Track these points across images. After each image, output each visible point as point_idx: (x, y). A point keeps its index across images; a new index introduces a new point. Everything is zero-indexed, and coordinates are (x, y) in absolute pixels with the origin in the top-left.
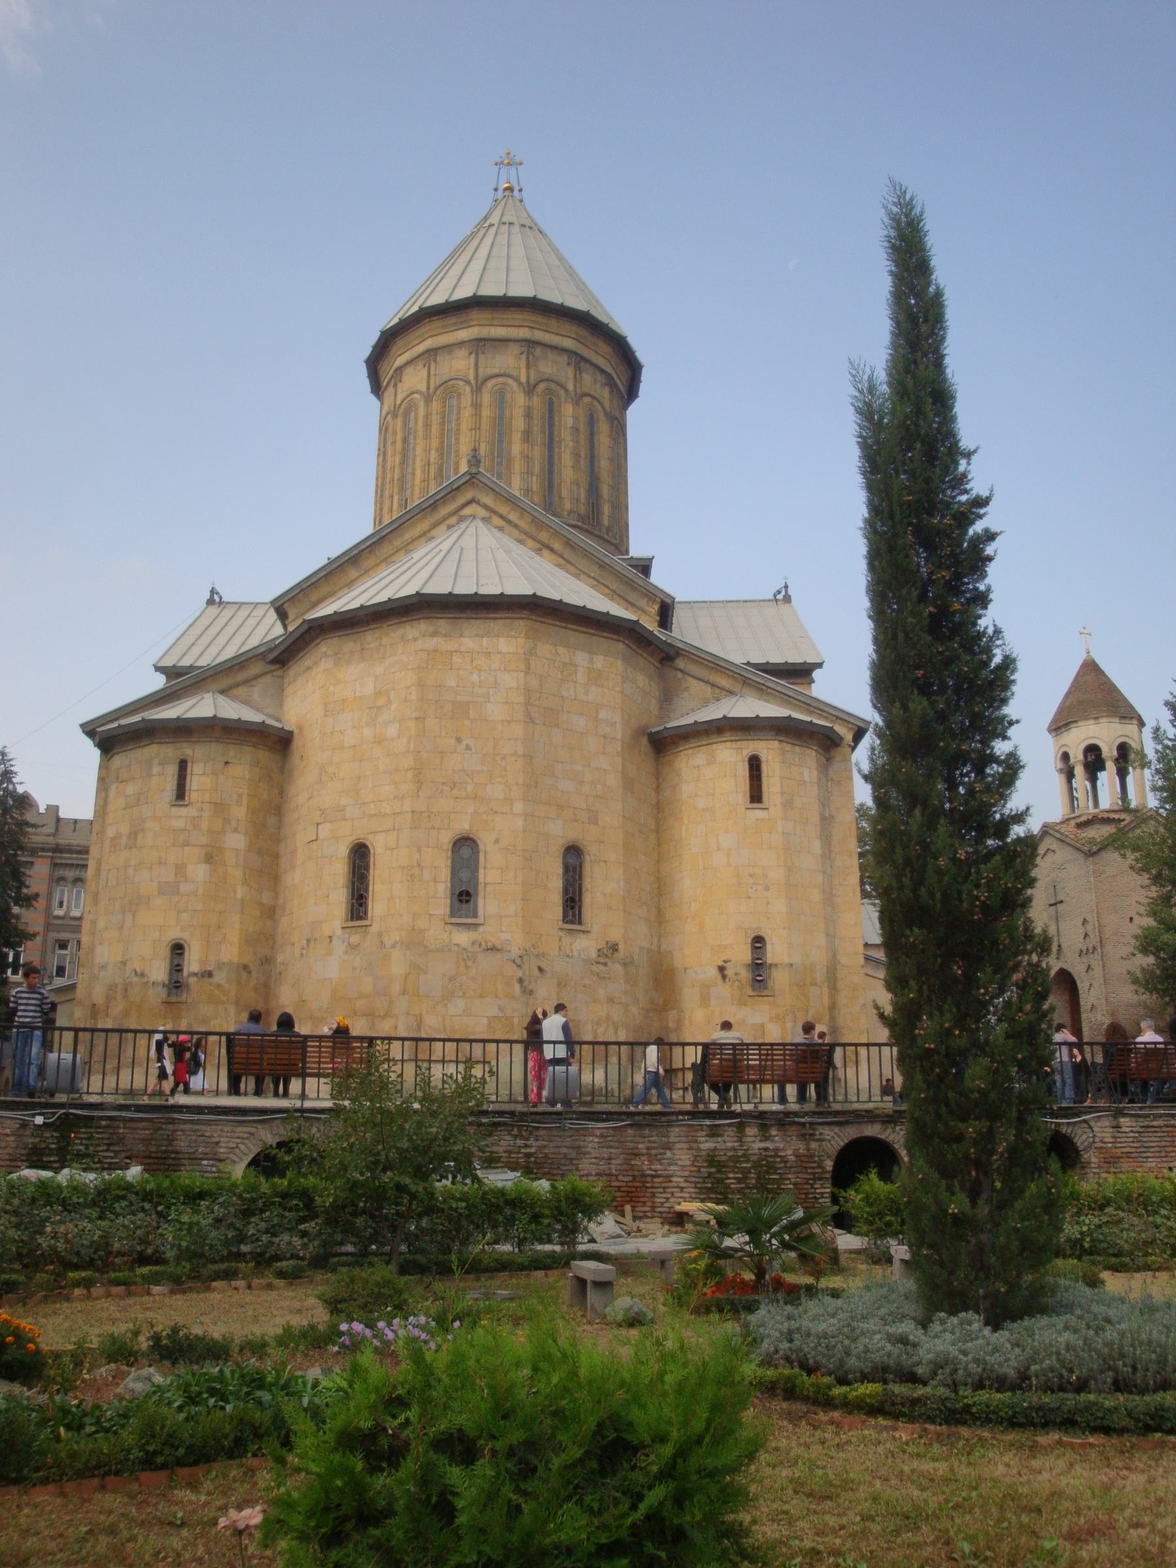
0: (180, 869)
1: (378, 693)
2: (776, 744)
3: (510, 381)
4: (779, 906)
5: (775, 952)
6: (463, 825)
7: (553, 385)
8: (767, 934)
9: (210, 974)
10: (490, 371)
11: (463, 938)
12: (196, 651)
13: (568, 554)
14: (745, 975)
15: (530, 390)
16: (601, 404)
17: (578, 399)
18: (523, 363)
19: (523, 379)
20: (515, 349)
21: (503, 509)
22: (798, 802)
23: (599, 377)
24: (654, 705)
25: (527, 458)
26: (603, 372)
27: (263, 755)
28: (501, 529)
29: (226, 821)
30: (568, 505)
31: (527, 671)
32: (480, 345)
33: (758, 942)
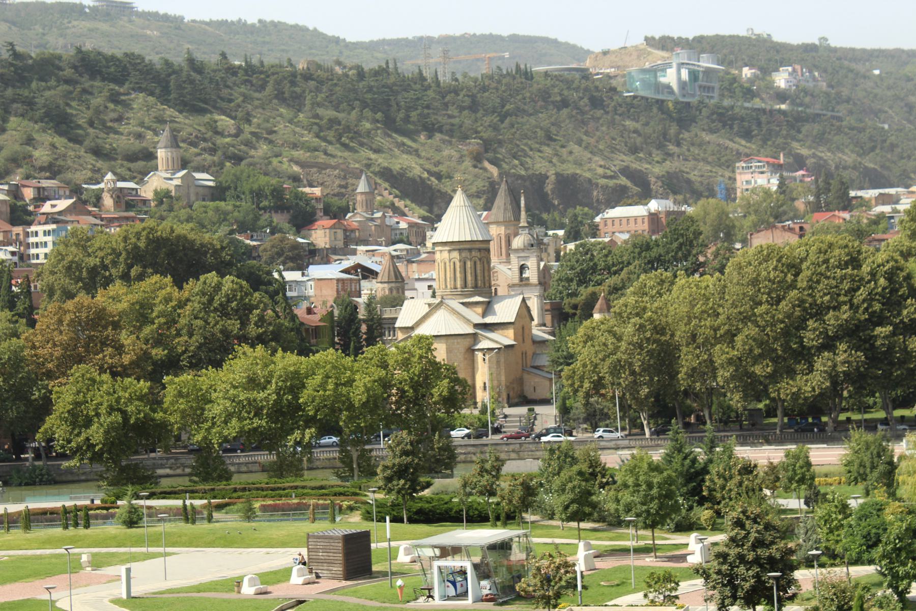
15: (460, 261)
17: (471, 260)
32: (450, 251)
33: (485, 384)
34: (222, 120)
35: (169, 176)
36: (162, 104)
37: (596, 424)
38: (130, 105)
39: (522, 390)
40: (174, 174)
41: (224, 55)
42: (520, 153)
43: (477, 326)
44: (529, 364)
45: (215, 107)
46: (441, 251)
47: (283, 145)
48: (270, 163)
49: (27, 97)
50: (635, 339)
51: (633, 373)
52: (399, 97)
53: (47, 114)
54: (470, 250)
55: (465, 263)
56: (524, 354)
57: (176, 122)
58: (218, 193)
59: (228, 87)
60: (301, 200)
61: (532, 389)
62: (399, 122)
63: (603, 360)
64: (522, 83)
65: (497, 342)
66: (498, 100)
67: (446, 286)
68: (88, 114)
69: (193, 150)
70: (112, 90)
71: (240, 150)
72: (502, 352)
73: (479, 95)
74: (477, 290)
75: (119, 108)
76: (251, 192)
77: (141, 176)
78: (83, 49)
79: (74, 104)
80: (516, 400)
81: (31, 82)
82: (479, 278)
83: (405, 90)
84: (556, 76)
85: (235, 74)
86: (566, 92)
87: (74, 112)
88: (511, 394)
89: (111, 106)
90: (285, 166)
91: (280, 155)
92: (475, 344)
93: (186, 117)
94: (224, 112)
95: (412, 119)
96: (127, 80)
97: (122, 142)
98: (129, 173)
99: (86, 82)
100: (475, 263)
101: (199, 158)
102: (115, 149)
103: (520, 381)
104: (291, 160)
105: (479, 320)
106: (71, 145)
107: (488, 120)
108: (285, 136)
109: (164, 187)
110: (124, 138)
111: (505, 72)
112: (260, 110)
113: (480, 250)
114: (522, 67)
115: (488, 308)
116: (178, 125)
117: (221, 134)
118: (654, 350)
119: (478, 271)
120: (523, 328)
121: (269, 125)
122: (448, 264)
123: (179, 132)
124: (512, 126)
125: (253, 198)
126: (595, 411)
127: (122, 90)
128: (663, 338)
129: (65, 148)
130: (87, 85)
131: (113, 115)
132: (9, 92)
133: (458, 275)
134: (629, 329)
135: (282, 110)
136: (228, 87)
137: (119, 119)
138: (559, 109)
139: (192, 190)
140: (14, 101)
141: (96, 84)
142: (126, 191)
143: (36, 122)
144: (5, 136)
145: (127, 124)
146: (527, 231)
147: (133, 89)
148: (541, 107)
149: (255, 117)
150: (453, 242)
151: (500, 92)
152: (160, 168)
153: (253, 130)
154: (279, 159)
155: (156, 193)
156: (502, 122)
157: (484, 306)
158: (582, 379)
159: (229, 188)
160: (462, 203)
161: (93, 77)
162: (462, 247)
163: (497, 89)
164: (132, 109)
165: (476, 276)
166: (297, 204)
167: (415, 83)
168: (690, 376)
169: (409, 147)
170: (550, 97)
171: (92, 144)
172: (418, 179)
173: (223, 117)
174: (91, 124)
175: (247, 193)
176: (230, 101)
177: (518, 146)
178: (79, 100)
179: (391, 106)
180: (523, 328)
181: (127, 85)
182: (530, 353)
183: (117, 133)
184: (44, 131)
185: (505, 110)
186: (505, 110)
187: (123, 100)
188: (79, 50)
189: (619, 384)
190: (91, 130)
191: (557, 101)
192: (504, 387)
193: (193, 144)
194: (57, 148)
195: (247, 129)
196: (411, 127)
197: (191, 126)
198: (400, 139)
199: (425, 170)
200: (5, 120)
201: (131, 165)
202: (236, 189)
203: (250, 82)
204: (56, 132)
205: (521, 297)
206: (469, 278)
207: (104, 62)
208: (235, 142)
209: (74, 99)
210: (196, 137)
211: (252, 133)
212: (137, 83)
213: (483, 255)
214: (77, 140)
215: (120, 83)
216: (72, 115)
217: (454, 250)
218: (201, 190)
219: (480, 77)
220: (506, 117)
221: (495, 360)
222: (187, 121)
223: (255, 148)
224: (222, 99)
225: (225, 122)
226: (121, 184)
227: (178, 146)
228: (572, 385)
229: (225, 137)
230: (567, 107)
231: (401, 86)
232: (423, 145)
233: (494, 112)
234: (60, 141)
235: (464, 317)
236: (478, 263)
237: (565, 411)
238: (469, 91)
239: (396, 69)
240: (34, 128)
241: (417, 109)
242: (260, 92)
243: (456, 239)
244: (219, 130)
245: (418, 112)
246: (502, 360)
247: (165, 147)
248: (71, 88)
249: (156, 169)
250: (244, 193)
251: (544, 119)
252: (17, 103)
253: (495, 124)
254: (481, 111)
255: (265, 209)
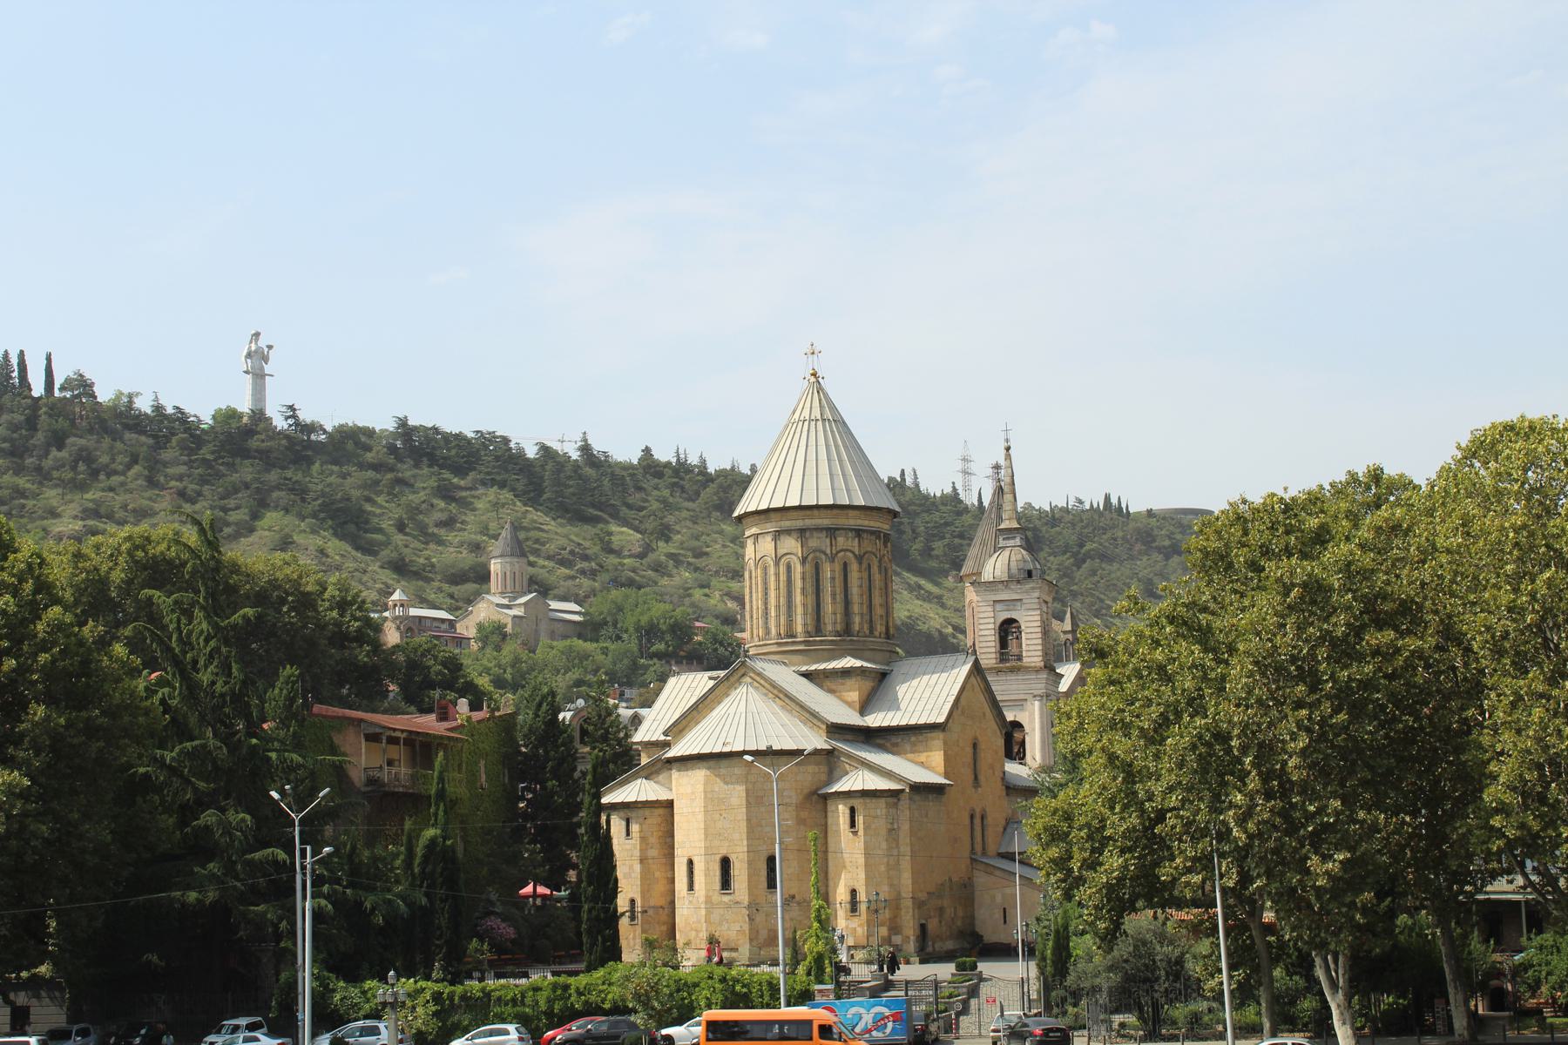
0: (631, 867)
1: (693, 793)
2: (861, 800)
3: (793, 557)
4: (862, 876)
5: (862, 896)
6: (723, 852)
7: (818, 554)
8: (857, 888)
9: (646, 912)
10: (785, 551)
11: (726, 899)
12: (679, 686)
13: (787, 700)
14: (848, 906)
15: (804, 561)
16: (851, 551)
17: (832, 559)
18: (799, 545)
19: (800, 555)
20: (795, 535)
21: (758, 679)
22: (873, 826)
23: (850, 534)
24: (824, 777)
25: (804, 605)
26: (851, 530)
27: (661, 811)
28: (756, 688)
29: (647, 844)
30: (830, 628)
31: (746, 782)
32: (777, 535)
33: (853, 892)
34: (622, 533)
35: (505, 602)
36: (525, 505)
37: (1156, 1007)
38: (472, 503)
39: (973, 917)
40: (515, 598)
41: (647, 451)
42: (1104, 611)
43: (836, 730)
44: (992, 848)
45: (615, 516)
46: (756, 536)
47: (716, 572)
48: (690, 595)
49: (297, 481)
50: (1287, 640)
51: (1277, 785)
52: (918, 522)
53: (325, 507)
54: (832, 532)
55: (817, 568)
56: (978, 819)
57: (543, 530)
58: (589, 629)
59: (640, 489)
60: (721, 644)
61: (998, 915)
62: (915, 555)
63: (1155, 737)
64: (1111, 519)
65: (888, 774)
66: (1074, 537)
67: (767, 631)
68: (397, 513)
69: (564, 571)
70: (444, 480)
71: (643, 577)
72: (904, 802)
73: (1044, 529)
74: (847, 639)
75: (453, 507)
76: (638, 629)
77: (461, 605)
78: (410, 423)
79: (380, 500)
80: (950, 945)
81: (313, 463)
82: (856, 608)
83: (928, 511)
84: (1164, 518)
85: (659, 475)
86: (1179, 537)
87: (378, 511)
88: (933, 925)
89: (442, 504)
90: (712, 602)
91: (708, 586)
92: (831, 780)
93: (562, 525)
94: (625, 523)
95: (935, 553)
96: (475, 469)
97: (452, 554)
98: (449, 601)
99: (406, 471)
100: (845, 565)
101: (570, 583)
102: (433, 566)
103: (965, 893)
104: (727, 594)
105: (852, 718)
106: (354, 553)
107: (1054, 561)
108: (722, 560)
109: (495, 617)
110: (452, 550)
111: (1088, 507)
112: (689, 524)
113: (858, 533)
114: (1114, 501)
115: (878, 686)
116: (545, 535)
117: (618, 553)
118: (1367, 684)
119: (855, 591)
120: (975, 746)
121: (697, 543)
122: (772, 570)
123: (543, 544)
124: (1094, 572)
125: (640, 641)
126: (1152, 967)
127: (462, 483)
128: (1413, 643)
129: (342, 556)
130: (408, 474)
131: (443, 516)
132: (273, 476)
133: (798, 598)
134: (1265, 604)
135: (724, 527)
136: (640, 489)
137: (449, 523)
138: (1167, 557)
139: (543, 627)
140: (278, 487)
141: (420, 472)
142: (428, 623)
143: (303, 518)
144: (251, 539)
145: (461, 530)
146: (1018, 541)
147: (484, 483)
148: (1140, 552)
149: (679, 532)
150: (784, 509)
151: (1078, 528)
152: (493, 591)
153: (673, 551)
154: (706, 591)
155: (480, 627)
156: (1079, 568)
157: (868, 685)
158: (1098, 840)
159: (606, 623)
160: (817, 413)
161: (417, 465)
162: (809, 523)
163: (1073, 525)
164: (474, 510)
165: (847, 603)
166: (716, 650)
167: (943, 504)
168: (1533, 797)
169: (927, 592)
170: (1154, 541)
171: (394, 555)
172: (936, 635)
173: (624, 529)
174: (401, 527)
175: (631, 630)
176: (641, 509)
177: (1102, 601)
178: (389, 494)
179: (905, 532)
180: (975, 746)
181: (472, 475)
182: (996, 818)
183: (440, 542)
184: (313, 532)
185: (1083, 551)
186: (1083, 551)
187: (466, 497)
188: (403, 423)
189: (1224, 835)
190: (399, 539)
191: (1164, 547)
192: (909, 903)
193: (563, 563)
194: (327, 556)
195: (663, 547)
196: (933, 564)
197: (566, 536)
198: (914, 579)
199: (949, 623)
200: (255, 516)
201: (455, 589)
202: (615, 625)
203: (683, 490)
204: (336, 535)
205: (974, 657)
206: (828, 607)
207: (442, 443)
208: (637, 565)
209: (379, 493)
210: (572, 552)
211: (671, 556)
212: (488, 473)
213: (868, 545)
214: (369, 550)
215: (460, 471)
216: (374, 514)
217: (788, 532)
218: (560, 628)
219: (1048, 509)
220: (1084, 561)
221: (881, 825)
222: (560, 530)
223: (670, 576)
224: (630, 507)
225: (623, 535)
226: (414, 612)
227: (523, 554)
228: (1062, 863)
229: (624, 557)
230: (1180, 554)
231: (921, 505)
232: (951, 590)
233: (1065, 553)
234: (335, 546)
235: (802, 706)
236: (854, 566)
237: (1058, 963)
238: (1030, 521)
239: (917, 485)
240: (299, 526)
241: (944, 538)
242: (693, 501)
243: (793, 501)
244: (615, 546)
245: (946, 541)
246: (906, 827)
247: (501, 556)
248: (378, 476)
249: (488, 592)
250: (626, 631)
251: (1145, 565)
252: (279, 489)
253: (1067, 568)
254: (1047, 549)
255: (659, 656)
